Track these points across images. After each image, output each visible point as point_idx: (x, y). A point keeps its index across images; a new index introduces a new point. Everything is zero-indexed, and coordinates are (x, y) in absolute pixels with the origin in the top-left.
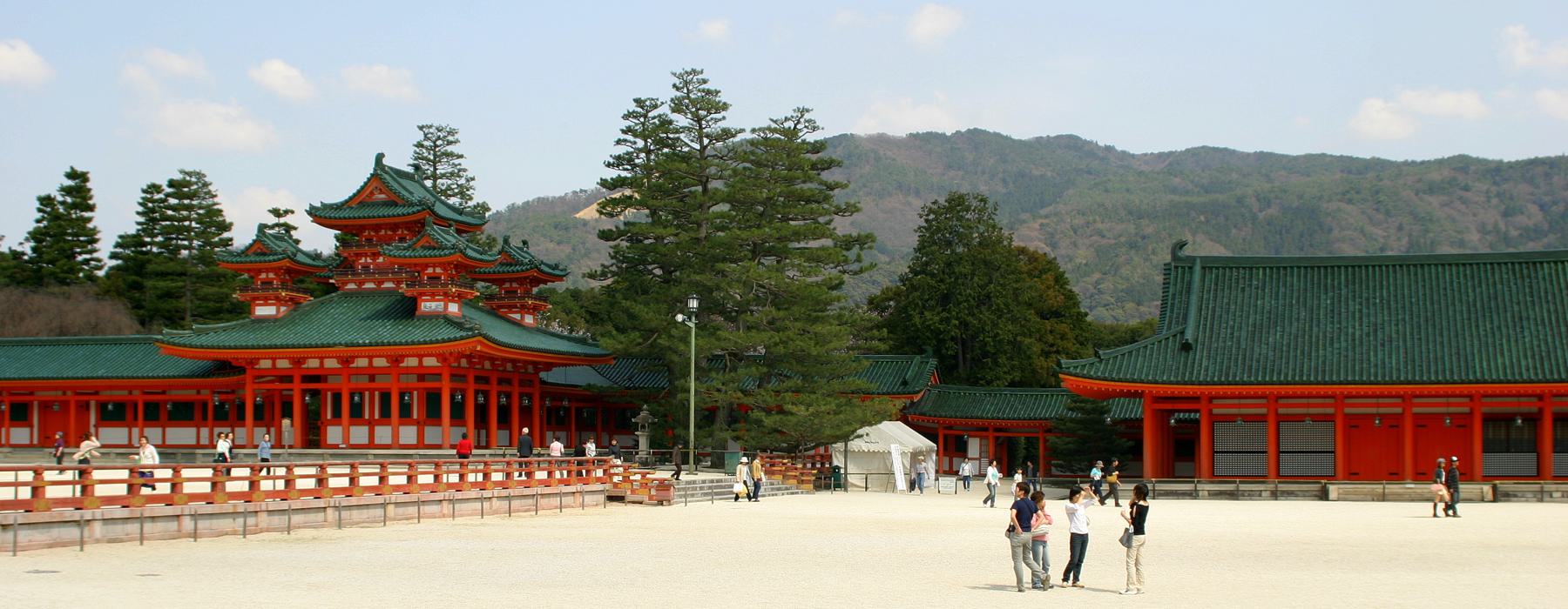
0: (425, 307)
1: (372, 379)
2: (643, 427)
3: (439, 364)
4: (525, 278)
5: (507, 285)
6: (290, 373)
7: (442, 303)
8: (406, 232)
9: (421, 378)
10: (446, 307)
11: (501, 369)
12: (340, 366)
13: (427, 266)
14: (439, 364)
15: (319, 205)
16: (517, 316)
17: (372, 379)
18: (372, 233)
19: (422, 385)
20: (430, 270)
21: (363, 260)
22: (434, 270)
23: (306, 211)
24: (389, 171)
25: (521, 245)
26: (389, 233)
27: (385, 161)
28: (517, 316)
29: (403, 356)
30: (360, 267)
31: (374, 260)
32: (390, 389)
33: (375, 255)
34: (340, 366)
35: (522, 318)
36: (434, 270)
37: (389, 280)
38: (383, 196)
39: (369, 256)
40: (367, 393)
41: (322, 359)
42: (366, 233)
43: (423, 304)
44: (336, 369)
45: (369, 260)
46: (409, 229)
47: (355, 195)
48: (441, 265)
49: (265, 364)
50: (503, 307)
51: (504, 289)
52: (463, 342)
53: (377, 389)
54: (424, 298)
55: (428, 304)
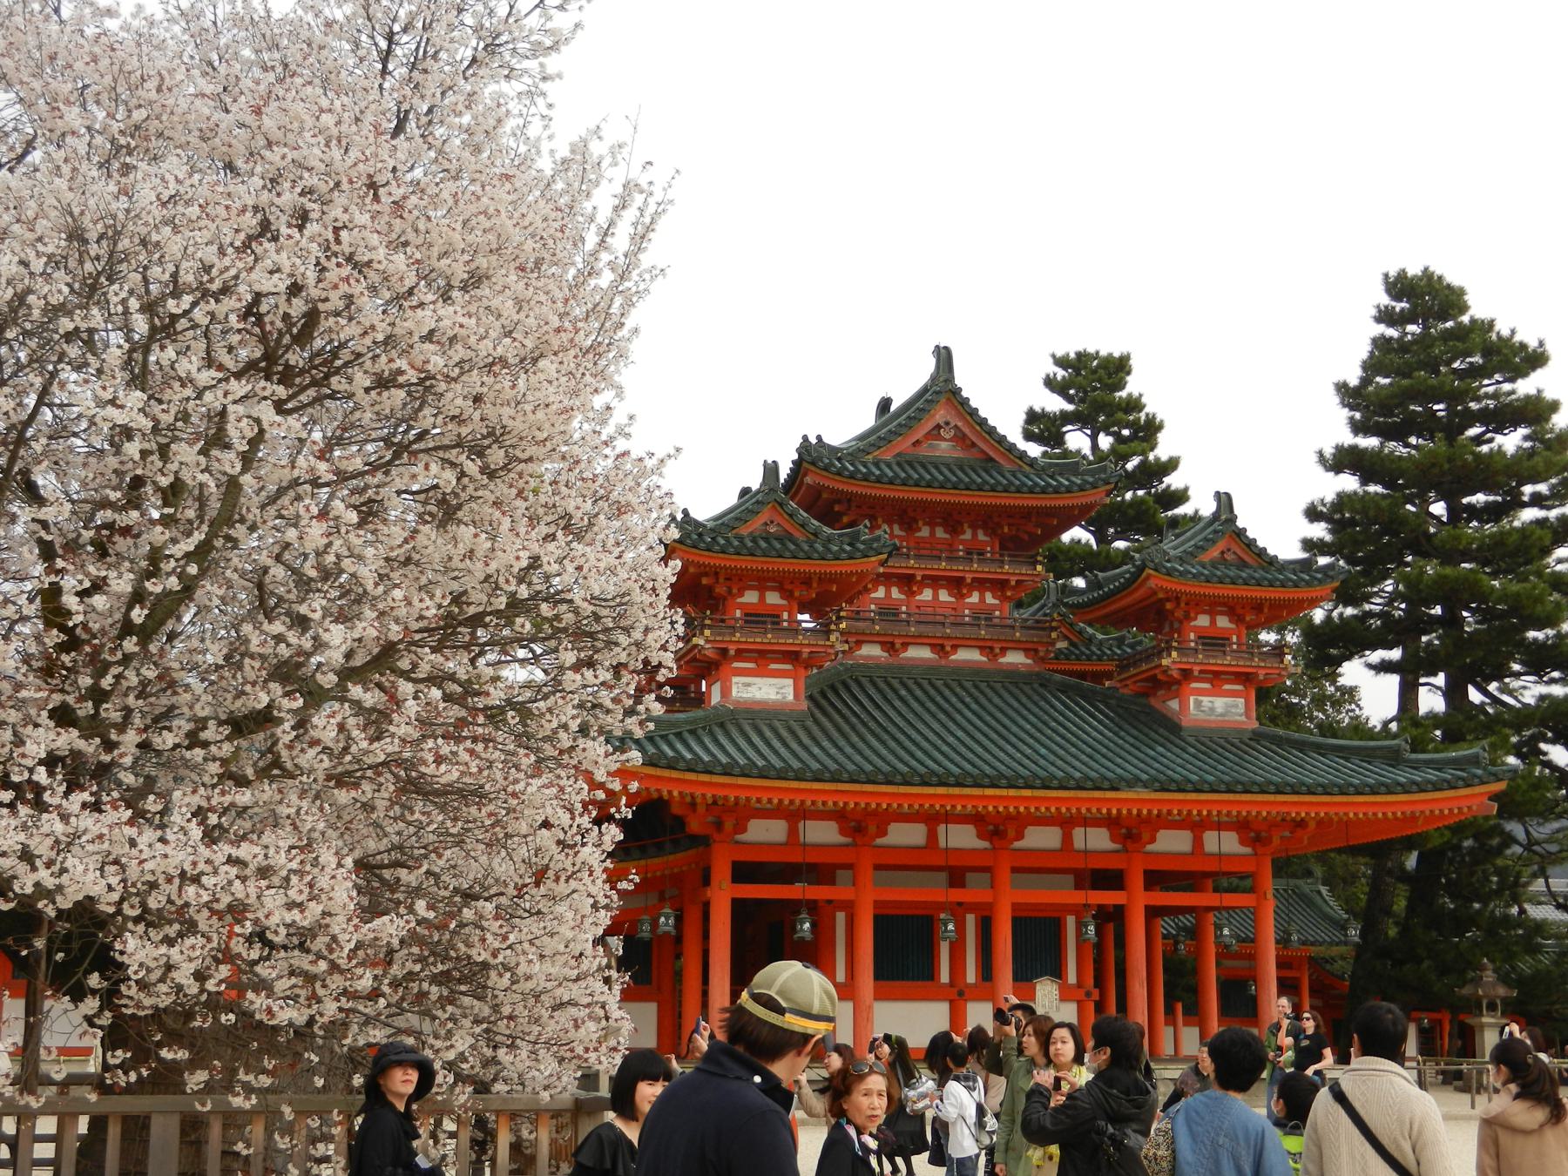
0: (1198, 704)
2: (1492, 1007)
8: (981, 536)
22: (1213, 622)
26: (940, 533)
34: (984, 844)
40: (971, 919)
43: (1192, 699)
44: (974, 850)
46: (992, 530)
49: (765, 832)
53: (971, 907)
55: (1206, 700)
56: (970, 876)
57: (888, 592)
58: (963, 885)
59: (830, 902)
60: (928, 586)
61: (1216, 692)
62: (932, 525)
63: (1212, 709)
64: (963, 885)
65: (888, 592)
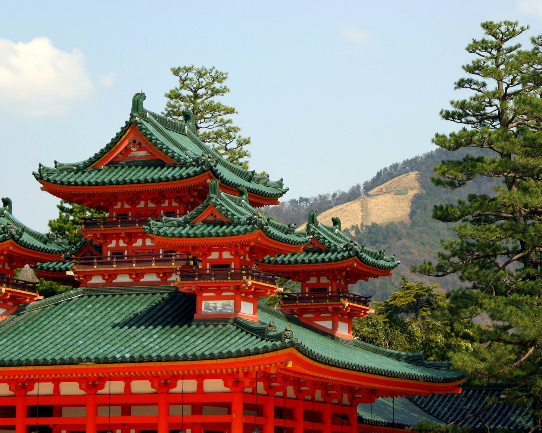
1: (126, 410)
3: (228, 390)
4: (340, 271)
5: (313, 280)
6: (9, 403)
7: (232, 302)
8: (174, 204)
9: (197, 409)
10: (237, 308)
11: (309, 397)
12: (82, 392)
13: (210, 249)
14: (228, 390)
15: (52, 166)
16: (328, 324)
17: (126, 410)
18: (127, 206)
19: (199, 419)
20: (215, 255)
21: (113, 244)
22: (220, 255)
23: (34, 174)
24: (152, 118)
25: (331, 224)
26: (151, 205)
27: (147, 105)
28: (328, 324)
29: (175, 378)
30: (109, 253)
31: (129, 243)
32: (156, 425)
33: (131, 237)
34: (82, 392)
35: (335, 327)
36: (220, 255)
37: (151, 271)
38: (143, 153)
39: (123, 239)
41: (57, 382)
42: (119, 206)
43: (204, 303)
45: (122, 244)
46: (179, 199)
47: (103, 152)
48: (231, 248)
50: (306, 311)
51: (309, 285)
52: (267, 355)
54: (205, 294)
55: (212, 303)
56: (205, 408)
57: (118, 243)
58: (201, 413)
59: (55, 425)
60: (140, 237)
61: (219, 297)
62: (146, 201)
63: (215, 308)
64: (201, 413)
65: (118, 243)
